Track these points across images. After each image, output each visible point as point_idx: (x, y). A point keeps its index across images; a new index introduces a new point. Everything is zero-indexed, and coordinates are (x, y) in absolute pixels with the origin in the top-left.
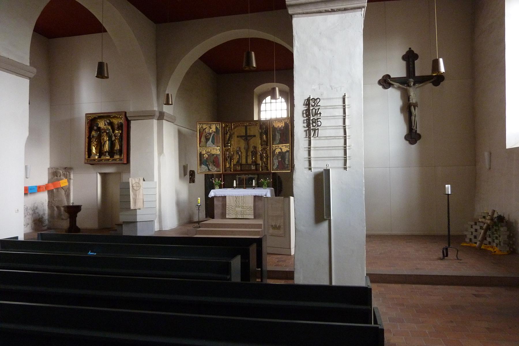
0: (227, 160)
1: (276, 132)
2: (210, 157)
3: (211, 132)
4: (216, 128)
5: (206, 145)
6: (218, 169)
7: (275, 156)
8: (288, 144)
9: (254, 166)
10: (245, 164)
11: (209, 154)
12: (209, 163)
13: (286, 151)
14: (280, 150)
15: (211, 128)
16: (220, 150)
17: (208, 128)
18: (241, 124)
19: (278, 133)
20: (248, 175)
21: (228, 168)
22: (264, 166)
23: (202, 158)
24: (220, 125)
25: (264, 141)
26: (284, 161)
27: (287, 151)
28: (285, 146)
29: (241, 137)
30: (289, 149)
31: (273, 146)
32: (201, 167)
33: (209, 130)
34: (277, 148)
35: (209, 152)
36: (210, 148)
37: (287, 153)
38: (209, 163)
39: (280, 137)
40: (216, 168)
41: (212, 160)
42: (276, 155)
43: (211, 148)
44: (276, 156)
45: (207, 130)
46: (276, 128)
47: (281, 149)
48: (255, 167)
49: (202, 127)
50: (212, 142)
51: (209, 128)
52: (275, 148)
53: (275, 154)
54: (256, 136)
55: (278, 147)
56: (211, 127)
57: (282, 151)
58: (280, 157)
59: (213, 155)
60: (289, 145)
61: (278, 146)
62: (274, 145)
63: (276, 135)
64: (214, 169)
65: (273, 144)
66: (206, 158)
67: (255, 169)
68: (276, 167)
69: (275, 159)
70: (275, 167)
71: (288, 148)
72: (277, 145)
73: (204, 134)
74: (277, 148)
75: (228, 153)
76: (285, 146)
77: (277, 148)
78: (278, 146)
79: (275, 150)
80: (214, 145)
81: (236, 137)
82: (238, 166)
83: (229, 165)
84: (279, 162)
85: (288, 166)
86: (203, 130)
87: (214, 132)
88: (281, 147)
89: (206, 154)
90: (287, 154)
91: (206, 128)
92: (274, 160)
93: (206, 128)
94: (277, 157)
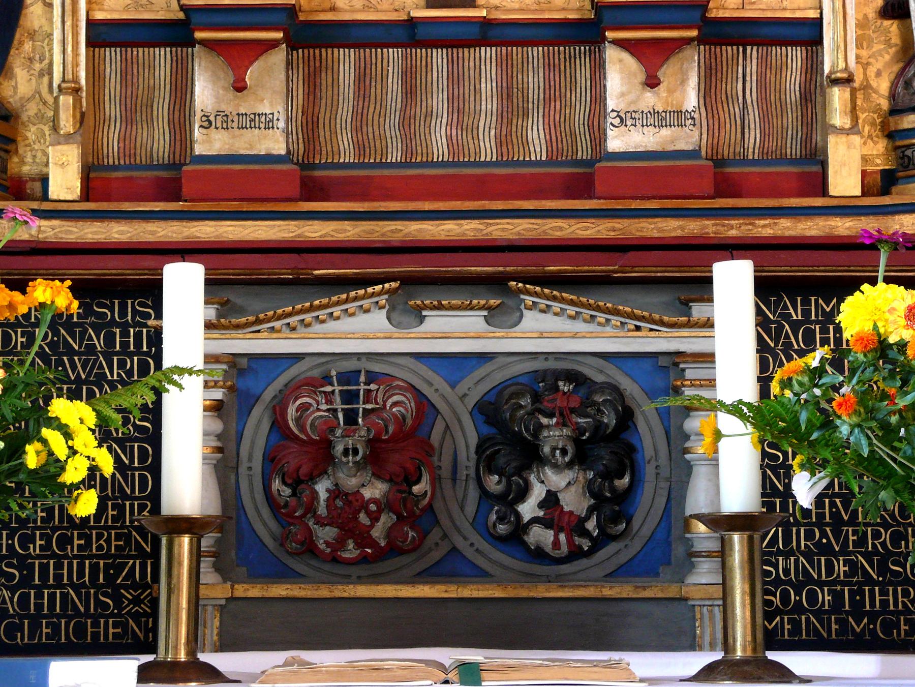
20: (493, 316)
48: (691, 99)
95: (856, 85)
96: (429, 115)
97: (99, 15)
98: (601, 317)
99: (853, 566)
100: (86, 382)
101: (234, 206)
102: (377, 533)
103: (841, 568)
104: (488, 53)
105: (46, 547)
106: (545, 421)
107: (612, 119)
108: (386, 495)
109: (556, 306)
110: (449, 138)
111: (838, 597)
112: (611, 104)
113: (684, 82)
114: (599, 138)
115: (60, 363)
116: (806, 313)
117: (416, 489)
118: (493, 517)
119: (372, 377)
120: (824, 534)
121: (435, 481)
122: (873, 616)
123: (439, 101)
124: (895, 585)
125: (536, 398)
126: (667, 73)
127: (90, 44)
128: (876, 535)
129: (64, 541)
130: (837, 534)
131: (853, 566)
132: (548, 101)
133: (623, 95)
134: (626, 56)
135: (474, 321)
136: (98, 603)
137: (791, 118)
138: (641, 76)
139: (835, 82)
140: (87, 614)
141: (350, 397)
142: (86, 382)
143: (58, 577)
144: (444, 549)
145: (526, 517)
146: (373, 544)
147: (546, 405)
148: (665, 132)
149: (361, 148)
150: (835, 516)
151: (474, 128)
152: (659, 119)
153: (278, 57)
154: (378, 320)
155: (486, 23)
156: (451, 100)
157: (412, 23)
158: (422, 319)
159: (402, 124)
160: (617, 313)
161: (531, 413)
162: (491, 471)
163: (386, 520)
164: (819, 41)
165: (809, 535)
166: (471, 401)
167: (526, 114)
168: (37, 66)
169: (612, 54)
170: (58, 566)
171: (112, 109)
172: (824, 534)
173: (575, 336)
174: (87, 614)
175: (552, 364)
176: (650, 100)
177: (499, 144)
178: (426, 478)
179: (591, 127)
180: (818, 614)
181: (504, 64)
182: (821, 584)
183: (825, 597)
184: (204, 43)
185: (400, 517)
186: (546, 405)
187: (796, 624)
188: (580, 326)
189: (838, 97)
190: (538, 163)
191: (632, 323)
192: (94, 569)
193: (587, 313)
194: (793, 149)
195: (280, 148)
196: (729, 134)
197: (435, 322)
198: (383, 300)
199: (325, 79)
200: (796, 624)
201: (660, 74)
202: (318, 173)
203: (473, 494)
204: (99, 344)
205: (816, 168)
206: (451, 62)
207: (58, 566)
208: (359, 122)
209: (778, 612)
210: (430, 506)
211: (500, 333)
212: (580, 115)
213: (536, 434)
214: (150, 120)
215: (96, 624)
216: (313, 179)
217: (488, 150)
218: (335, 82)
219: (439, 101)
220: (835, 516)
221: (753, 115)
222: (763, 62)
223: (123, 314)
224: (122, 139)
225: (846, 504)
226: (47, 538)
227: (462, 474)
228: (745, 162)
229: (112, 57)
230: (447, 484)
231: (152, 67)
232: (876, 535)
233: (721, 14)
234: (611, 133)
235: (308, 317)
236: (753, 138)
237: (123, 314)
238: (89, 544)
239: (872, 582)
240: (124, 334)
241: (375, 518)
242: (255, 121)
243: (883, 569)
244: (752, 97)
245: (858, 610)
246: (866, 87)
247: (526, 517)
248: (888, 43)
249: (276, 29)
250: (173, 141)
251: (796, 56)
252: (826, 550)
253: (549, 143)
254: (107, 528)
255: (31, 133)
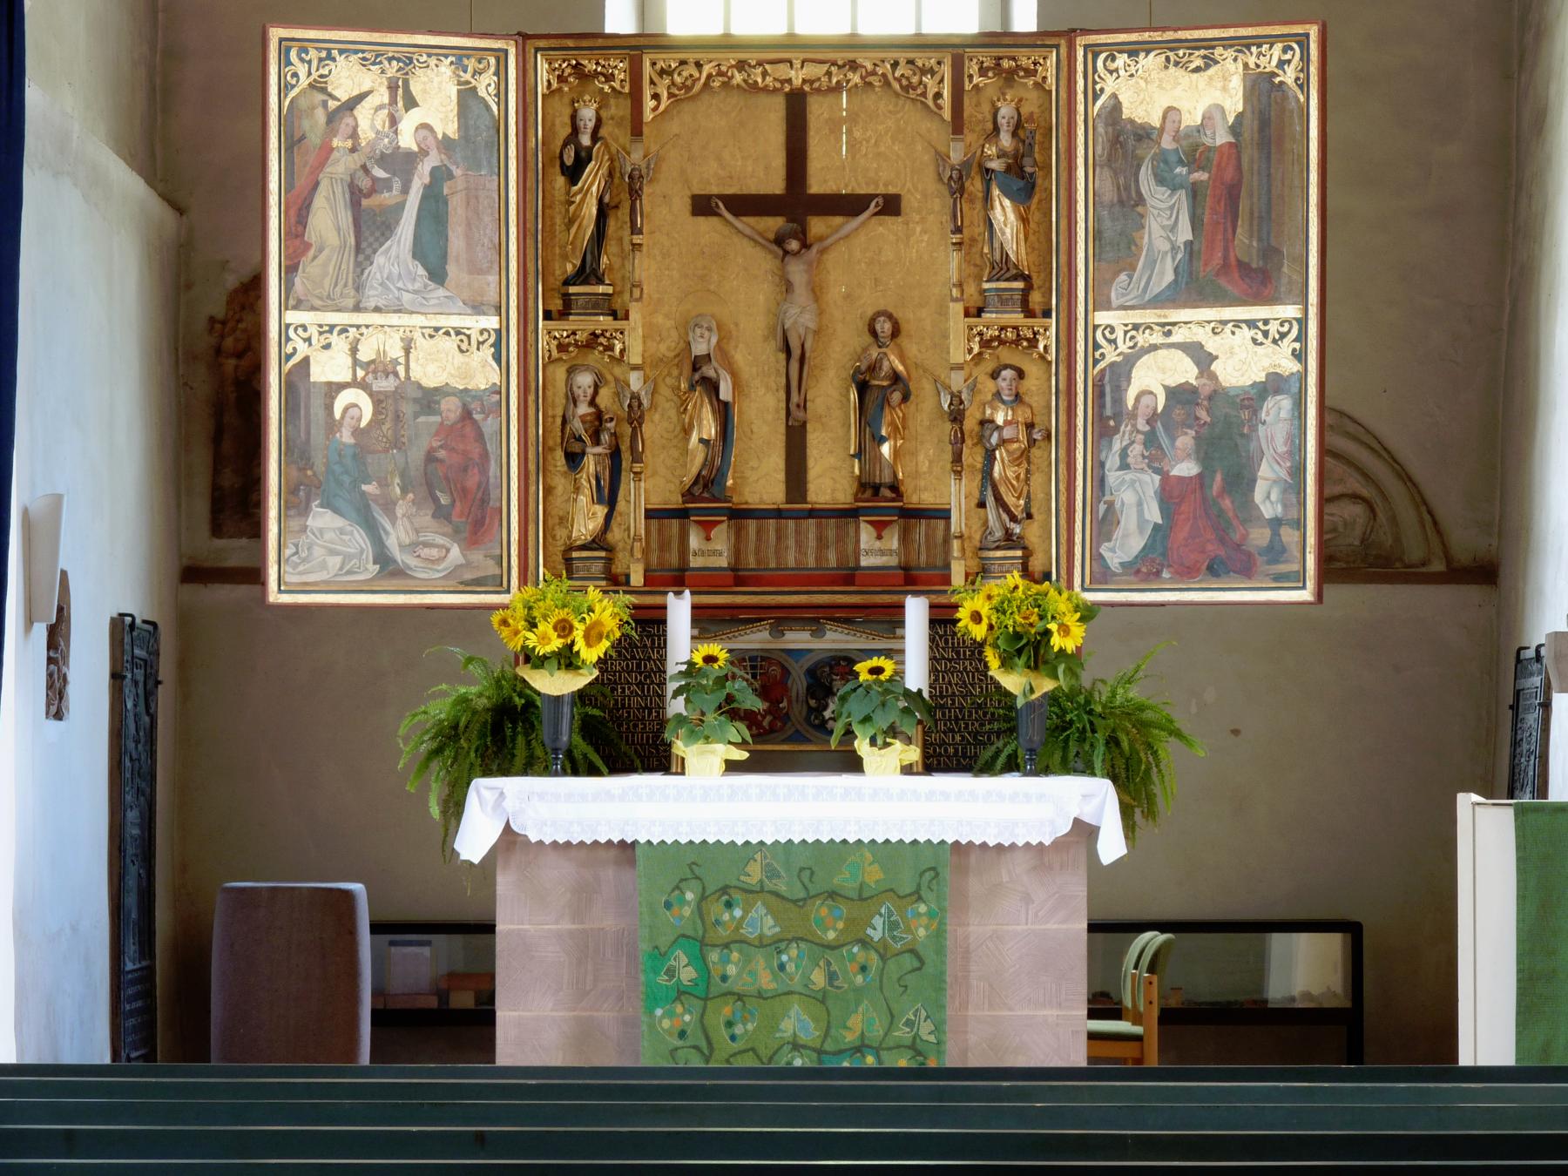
0: (574, 460)
1: (1146, 175)
2: (398, 418)
3: (407, 141)
4: (467, 96)
5: (358, 288)
6: (477, 556)
7: (1125, 428)
8: (1291, 311)
9: (879, 527)
10: (778, 514)
11: (385, 385)
12: (384, 484)
13: (1261, 377)
14: (1184, 371)
15: (411, 103)
16: (497, 345)
17: (383, 96)
18: (741, 65)
19: (1161, 181)
20: (815, 634)
21: (583, 548)
22: (999, 534)
23: (318, 436)
24: (502, 71)
25: (1003, 268)
26: (1241, 481)
27: (1274, 384)
28: (1246, 333)
29: (744, 205)
30: (1300, 356)
31: (1102, 318)
32: (294, 524)
33: (394, 122)
34: (1154, 348)
35: (389, 370)
36: (394, 319)
37: (1270, 403)
38: (384, 484)
39: (1185, 233)
40: (455, 551)
41: (416, 455)
42: (1133, 415)
43: (404, 320)
44: (1142, 425)
45: (368, 121)
46: (1144, 134)
47: (1202, 358)
48: (895, 544)
49: (319, 86)
50: (418, 253)
51: (393, 101)
52: (1123, 348)
53: (1119, 400)
54: (910, 202)
55: (1157, 338)
56: (415, 88)
57: (1213, 377)
58: (1186, 441)
59: (429, 399)
60: (1303, 322)
61: (1168, 328)
62: (1108, 306)
63: (1141, 200)
64: (434, 553)
65: (1103, 304)
66: (357, 432)
67: (893, 561)
68: (1136, 544)
69: (1124, 466)
70: (1127, 544)
71: (1288, 345)
72: (1149, 316)
73: (342, 165)
74: (1143, 339)
75: (585, 380)
76: (1251, 324)
77: (1154, 348)
78: (1168, 328)
79: (1130, 361)
80: (441, 292)
81: (682, 204)
82: (707, 527)
83: (601, 511)
84: (1171, 494)
85: (1289, 536)
86: (332, 118)
87: (446, 144)
88: (1202, 335)
89: (354, 383)
90: (1278, 409)
91: (361, 97)
92: (1113, 477)
93: (361, 97)
94: (1151, 440)
95: (966, 536)
96: (787, 548)
97: (649, 507)
98: (858, 634)
99: (963, 737)
100: (644, 659)
101: (706, 589)
102: (765, 723)
103: (958, 738)
104: (812, 521)
105: (628, 728)
106: (834, 677)
107: (862, 552)
108: (769, 708)
109: (840, 630)
110: (795, 557)
111: (956, 750)
112: (862, 546)
113: (892, 537)
114: (857, 560)
115: (633, 651)
116: (945, 631)
117: (781, 705)
118: (813, 717)
119: (763, 659)
120: (951, 724)
121: (790, 702)
122: (970, 758)
123: (791, 542)
124: (980, 745)
125: (831, 668)
126: (885, 533)
127: (646, 518)
128: (973, 724)
129: (635, 726)
130: (957, 724)
131: (963, 737)
132: (837, 542)
133: (867, 542)
134: (869, 526)
135: (806, 635)
136: (650, 751)
137: (939, 550)
138: (875, 534)
139: (956, 537)
140: (645, 756)
141: (753, 667)
142: (644, 659)
143: (633, 741)
144: (793, 729)
145: (827, 717)
146: (764, 728)
147: (835, 671)
148: (885, 558)
149: (758, 562)
150: (956, 717)
151: (806, 554)
152: (882, 553)
153: (724, 526)
154: (765, 635)
155: (812, 510)
156: (796, 541)
157: (779, 510)
158: (784, 635)
159: (776, 552)
160: (864, 632)
161: (829, 675)
162: (812, 698)
163: (769, 718)
164: (950, 518)
165: (945, 725)
166: (805, 667)
167: (828, 547)
168: (623, 527)
169: (863, 526)
170: (633, 736)
171: (654, 545)
172: (951, 724)
173: (847, 642)
174: (645, 756)
175: (839, 654)
176: (878, 544)
177: (817, 559)
178: (785, 700)
179: (855, 552)
180: (948, 757)
181: (819, 526)
182: (950, 745)
183: (951, 750)
184: (695, 521)
185: (775, 718)
186: (835, 671)
187: (939, 763)
188: (850, 638)
189: (956, 544)
190: (833, 569)
191: (871, 637)
192: (648, 738)
193: (853, 632)
194: (939, 562)
195: (725, 565)
196: (914, 556)
197: (789, 635)
198: (768, 627)
199: (743, 533)
200: (939, 763)
201: (883, 534)
202: (740, 573)
203: (805, 706)
204: (649, 644)
205: (946, 572)
206: (796, 525)
207: (633, 736)
208: (758, 551)
209: (932, 756)
210: (787, 714)
211: (817, 640)
212: (850, 548)
213: (831, 683)
214: (670, 553)
215: (649, 760)
216: (739, 576)
217: (811, 563)
218: (747, 534)
219: (791, 542)
220: (956, 717)
221: (923, 548)
222: (928, 526)
223: (658, 631)
224: (659, 558)
225: (960, 712)
226: (628, 724)
227: (801, 699)
228: (919, 568)
229: (654, 523)
230: (794, 703)
231: (671, 528)
232: (973, 724)
233: (910, 506)
234: (862, 558)
235: (736, 634)
236: (923, 558)
237: (658, 631)
238: (645, 727)
239: (970, 743)
240: (659, 639)
241: (764, 717)
242: (715, 553)
243: (975, 738)
244: (923, 540)
245: (964, 755)
246: (970, 538)
247: (827, 717)
248: (980, 518)
249: (724, 516)
250: (679, 559)
251: (941, 524)
252: (952, 731)
253: (837, 560)
254: (653, 721)
255: (620, 555)
